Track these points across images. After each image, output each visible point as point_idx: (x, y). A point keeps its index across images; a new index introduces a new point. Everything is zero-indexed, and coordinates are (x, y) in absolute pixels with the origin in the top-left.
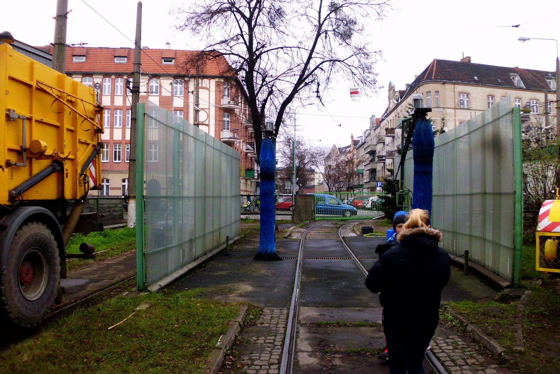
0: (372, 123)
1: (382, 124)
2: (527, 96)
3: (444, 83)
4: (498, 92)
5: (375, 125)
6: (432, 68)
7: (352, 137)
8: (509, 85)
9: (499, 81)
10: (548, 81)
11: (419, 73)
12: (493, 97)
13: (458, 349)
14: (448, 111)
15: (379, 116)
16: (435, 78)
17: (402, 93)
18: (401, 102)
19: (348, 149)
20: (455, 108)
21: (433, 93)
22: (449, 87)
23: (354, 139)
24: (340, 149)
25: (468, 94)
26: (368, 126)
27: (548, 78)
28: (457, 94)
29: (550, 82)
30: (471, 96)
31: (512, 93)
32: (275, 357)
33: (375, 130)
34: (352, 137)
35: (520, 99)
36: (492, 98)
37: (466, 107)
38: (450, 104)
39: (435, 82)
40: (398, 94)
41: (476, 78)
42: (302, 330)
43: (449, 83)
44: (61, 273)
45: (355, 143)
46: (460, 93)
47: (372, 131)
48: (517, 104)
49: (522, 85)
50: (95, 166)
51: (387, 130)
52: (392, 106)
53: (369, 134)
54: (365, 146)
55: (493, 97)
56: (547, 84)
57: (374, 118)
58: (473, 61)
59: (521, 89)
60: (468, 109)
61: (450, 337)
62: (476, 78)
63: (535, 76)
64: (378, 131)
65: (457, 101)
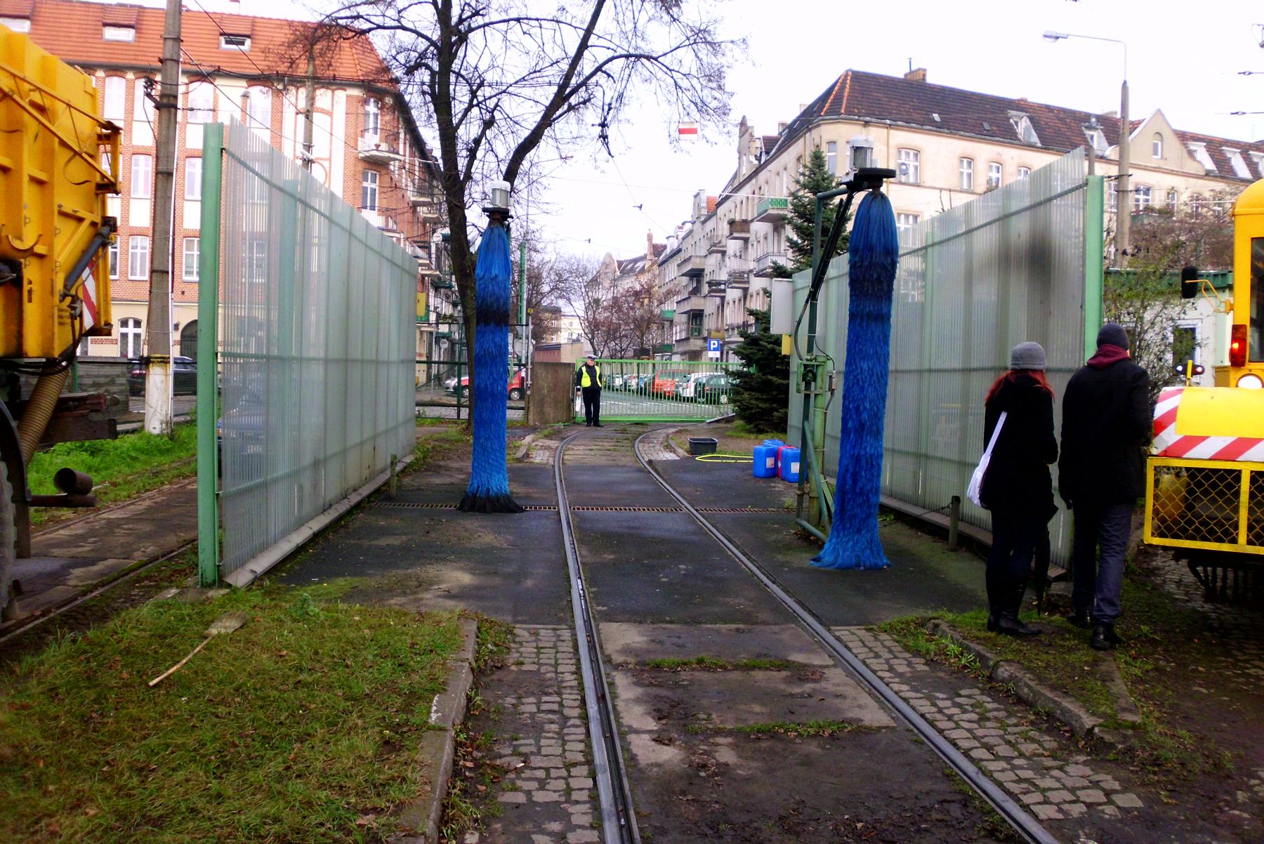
0: (697, 206)
1: (721, 211)
3: (867, 124)
4: (984, 151)
5: (704, 212)
6: (842, 88)
7: (650, 237)
8: (1006, 135)
9: (986, 126)
10: (1088, 133)
12: (971, 161)
13: (988, 719)
16: (849, 112)
17: (769, 142)
18: (767, 163)
19: (640, 265)
23: (655, 241)
24: (620, 263)
25: (917, 153)
26: (687, 213)
27: (1089, 128)
28: (893, 151)
29: (1092, 137)
30: (923, 156)
31: (1011, 156)
32: (575, 750)
33: (704, 223)
34: (650, 237)
36: (969, 163)
37: (912, 180)
40: (759, 144)
41: (936, 117)
42: (621, 679)
43: (876, 125)
44: (17, 544)
46: (899, 149)
47: (698, 224)
49: (1035, 139)
50: (95, 274)
51: (732, 223)
52: (746, 171)
53: (690, 233)
54: (682, 256)
55: (971, 161)
57: (703, 197)
58: (932, 79)
59: (1031, 146)
60: (917, 185)
61: (963, 692)
62: (936, 117)
63: (1061, 119)
64: (710, 225)
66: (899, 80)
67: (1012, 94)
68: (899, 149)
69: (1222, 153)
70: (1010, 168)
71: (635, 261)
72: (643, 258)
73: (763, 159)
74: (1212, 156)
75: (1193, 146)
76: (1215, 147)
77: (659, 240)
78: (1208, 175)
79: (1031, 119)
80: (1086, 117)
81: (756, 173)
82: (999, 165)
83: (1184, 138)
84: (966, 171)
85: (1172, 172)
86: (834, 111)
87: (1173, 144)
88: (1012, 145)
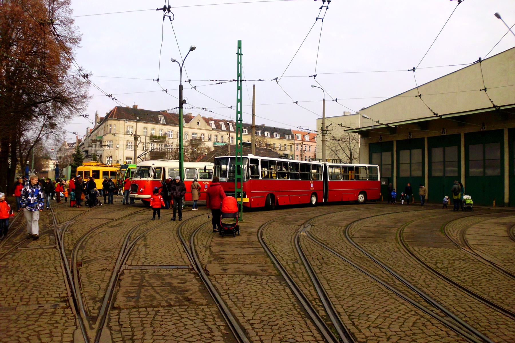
0: (87, 131)
2: (166, 128)
3: (119, 120)
4: (150, 126)
8: (157, 121)
11: (109, 112)
12: (147, 128)
14: (121, 135)
15: (92, 127)
17: (102, 119)
20: (124, 134)
21: (112, 126)
22: (122, 122)
24: (68, 144)
28: (126, 127)
31: (157, 127)
35: (162, 130)
38: (122, 131)
39: (114, 120)
48: (161, 132)
51: (92, 140)
55: (147, 128)
57: (89, 130)
59: (163, 124)
62: (138, 118)
63: (173, 117)
65: (126, 130)
66: (131, 108)
68: (128, 127)
69: (219, 123)
70: (157, 130)
71: (73, 144)
72: (75, 143)
74: (215, 125)
75: (210, 122)
76: (217, 122)
78: (213, 129)
79: (164, 117)
82: (154, 129)
83: (207, 121)
84: (145, 131)
85: (202, 129)
86: (111, 117)
87: (203, 123)
88: (158, 124)
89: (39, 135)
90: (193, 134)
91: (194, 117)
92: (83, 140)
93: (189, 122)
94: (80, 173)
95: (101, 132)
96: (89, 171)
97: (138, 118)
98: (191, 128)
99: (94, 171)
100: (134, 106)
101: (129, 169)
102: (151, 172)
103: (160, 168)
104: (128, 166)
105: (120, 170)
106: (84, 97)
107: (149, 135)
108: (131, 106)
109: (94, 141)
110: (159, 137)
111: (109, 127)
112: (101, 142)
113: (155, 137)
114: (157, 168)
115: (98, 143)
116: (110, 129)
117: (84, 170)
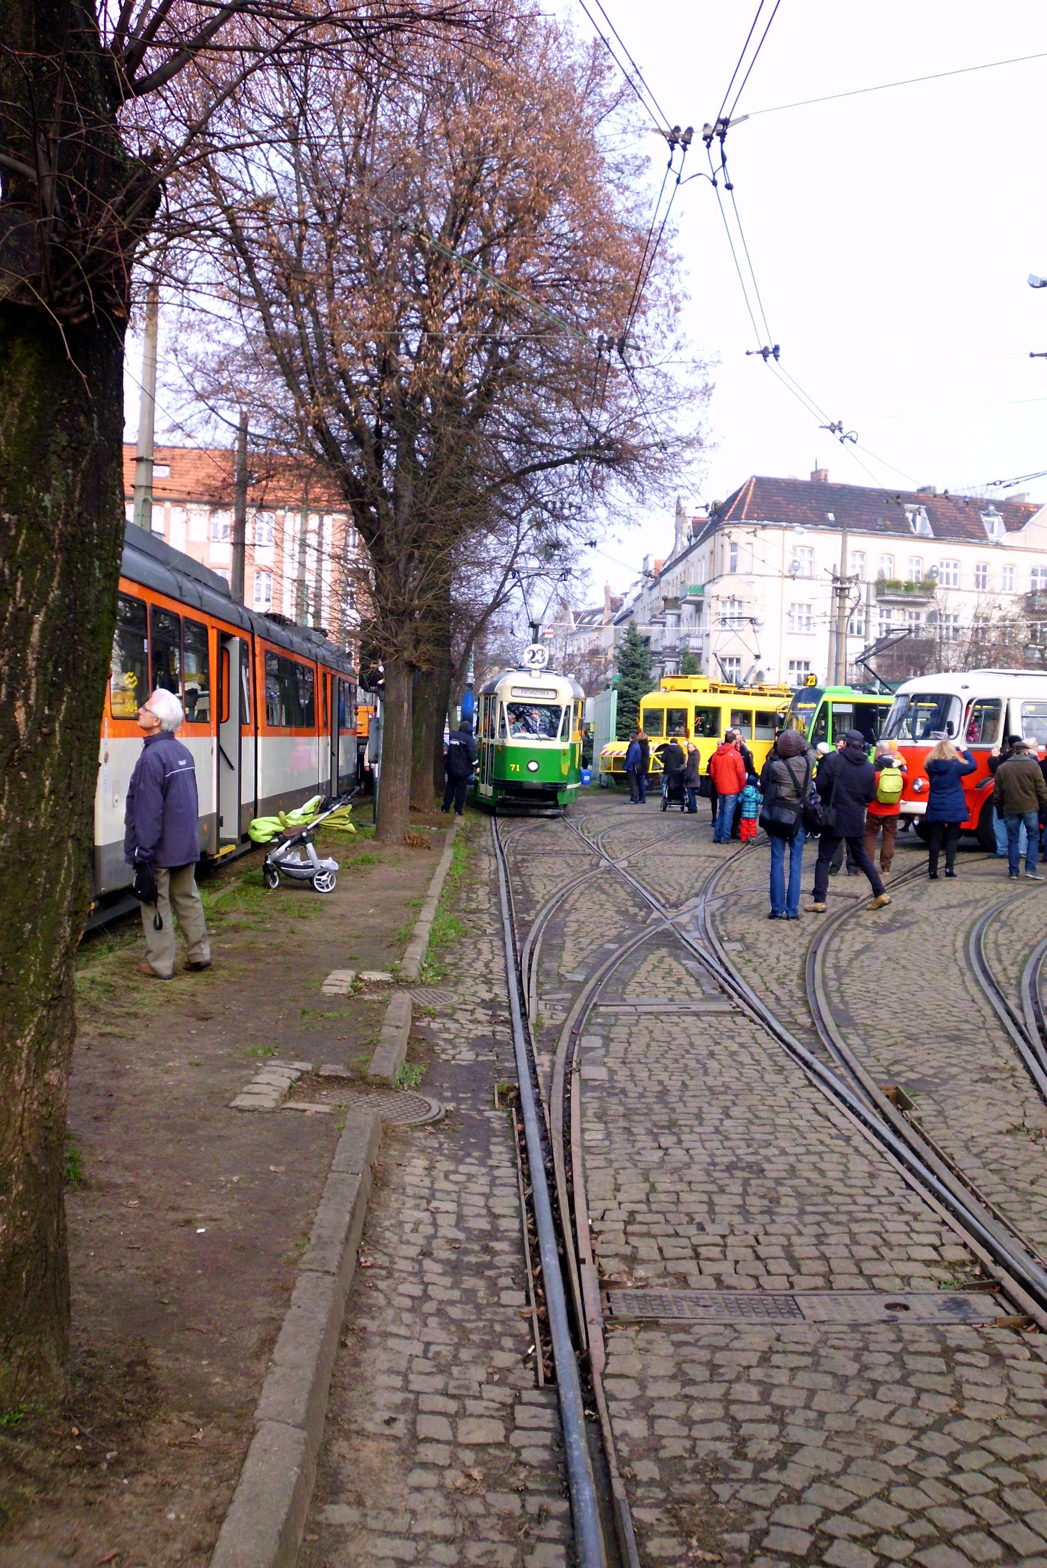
7: (607, 590)
8: (901, 528)
11: (723, 499)
17: (698, 525)
19: (598, 618)
25: (811, 551)
27: (988, 515)
40: (690, 523)
45: (615, 604)
48: (915, 568)
49: (929, 532)
51: (665, 599)
52: (680, 550)
56: (982, 528)
58: (833, 479)
59: (922, 538)
60: (810, 578)
62: (831, 516)
63: (961, 510)
65: (788, 562)
66: (805, 483)
67: (910, 487)
72: (600, 611)
73: (693, 541)
77: (616, 594)
80: (979, 506)
81: (685, 554)
82: (891, 557)
86: (736, 517)
89: (502, 585)
90: (1034, 573)
91: (1038, 507)
92: (628, 603)
93: (1019, 529)
94: (653, 718)
95: (697, 570)
96: (683, 713)
97: (831, 516)
98: (1027, 550)
99: (700, 711)
100: (816, 474)
101: (825, 704)
102: (956, 716)
103: (996, 702)
104: (820, 693)
105: (793, 706)
106: (689, 443)
107: (873, 578)
108: (806, 477)
109: (671, 603)
110: (909, 587)
111: (728, 553)
112: (698, 607)
113: (895, 585)
114: (981, 702)
115: (687, 609)
116: (734, 559)
117: (665, 707)
